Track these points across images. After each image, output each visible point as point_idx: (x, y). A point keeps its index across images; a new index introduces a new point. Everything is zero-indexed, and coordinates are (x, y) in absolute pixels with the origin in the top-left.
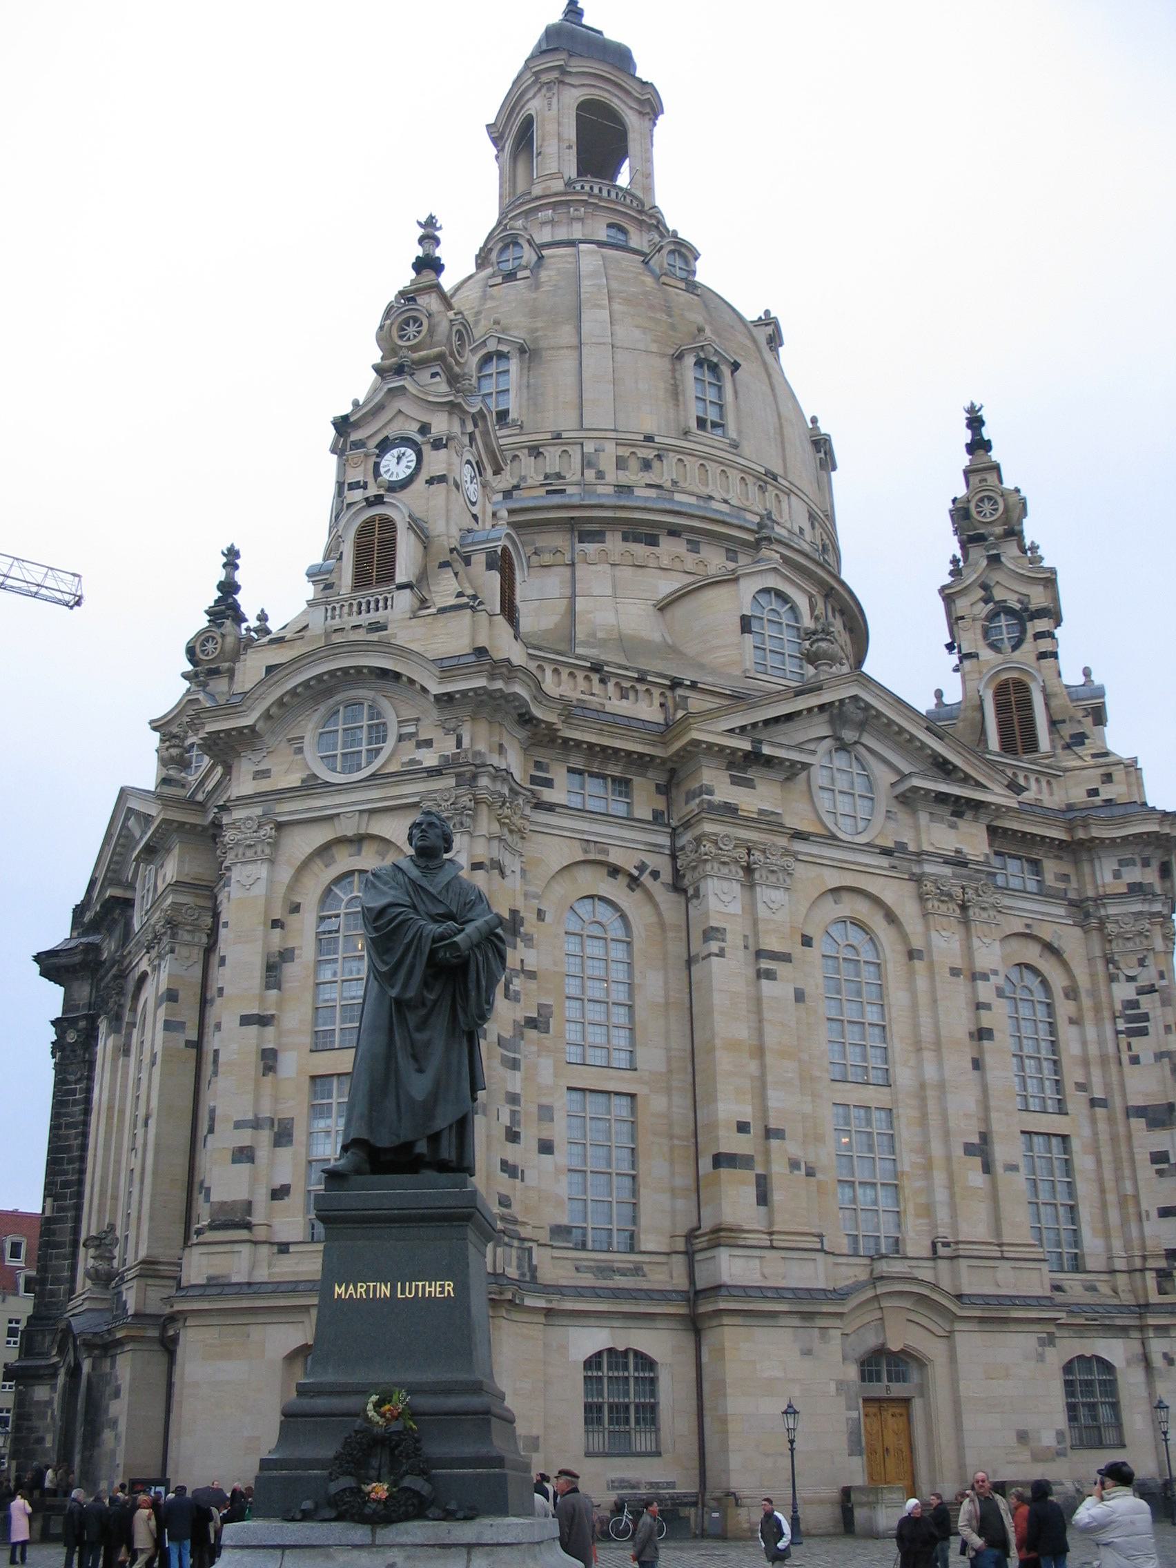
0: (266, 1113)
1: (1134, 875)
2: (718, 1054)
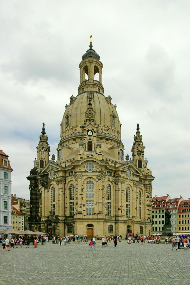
0: (82, 203)
1: (150, 183)
2: (119, 200)
